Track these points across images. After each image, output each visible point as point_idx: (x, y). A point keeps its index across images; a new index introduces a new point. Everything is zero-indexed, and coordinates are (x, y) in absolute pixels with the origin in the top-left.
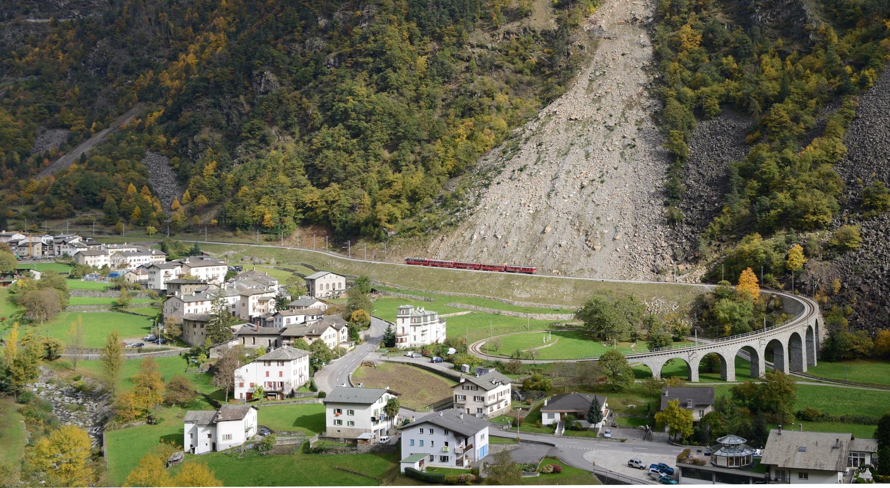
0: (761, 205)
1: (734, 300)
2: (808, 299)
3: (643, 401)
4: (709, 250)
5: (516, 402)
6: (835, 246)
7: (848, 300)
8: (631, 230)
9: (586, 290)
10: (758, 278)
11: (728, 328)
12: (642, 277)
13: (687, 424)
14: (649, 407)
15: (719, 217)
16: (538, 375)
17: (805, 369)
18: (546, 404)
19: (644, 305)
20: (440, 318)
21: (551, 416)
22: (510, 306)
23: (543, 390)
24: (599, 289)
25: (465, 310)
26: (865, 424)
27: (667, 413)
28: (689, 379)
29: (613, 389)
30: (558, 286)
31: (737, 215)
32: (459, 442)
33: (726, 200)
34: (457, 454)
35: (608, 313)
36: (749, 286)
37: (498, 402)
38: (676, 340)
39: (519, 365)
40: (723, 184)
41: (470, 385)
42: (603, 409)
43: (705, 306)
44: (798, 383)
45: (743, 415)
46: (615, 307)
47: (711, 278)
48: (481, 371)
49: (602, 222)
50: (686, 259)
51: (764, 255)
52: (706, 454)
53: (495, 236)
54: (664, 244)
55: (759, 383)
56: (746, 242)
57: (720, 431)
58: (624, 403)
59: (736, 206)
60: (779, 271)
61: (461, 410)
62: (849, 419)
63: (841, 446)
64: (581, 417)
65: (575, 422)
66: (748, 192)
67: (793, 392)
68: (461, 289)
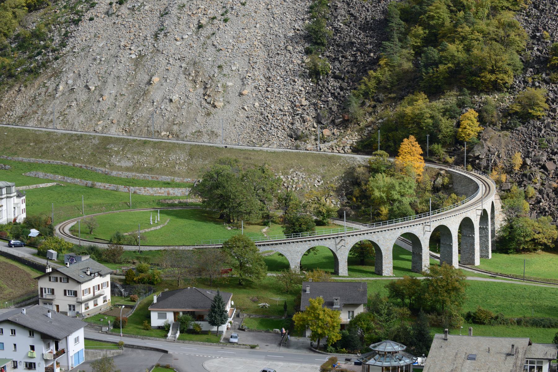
0: (427, 58)
1: (392, 175)
2: (483, 177)
3: (278, 299)
4: (362, 112)
5: (117, 298)
6: (516, 113)
7: (530, 179)
8: (262, 84)
9: (204, 158)
10: (423, 148)
11: (384, 210)
12: (276, 144)
13: (334, 327)
14: (285, 306)
15: (375, 71)
16: (144, 265)
17: (477, 262)
18: (155, 301)
19: (279, 179)
20: (17, 191)
21: (162, 316)
22: (107, 178)
23: (151, 284)
24: (221, 157)
25: (49, 181)
26: (544, 326)
27: (309, 313)
28: (336, 273)
29: (240, 284)
30: (168, 153)
31: (397, 69)
32: (48, 346)
33: (384, 50)
34: (46, 361)
35: (232, 188)
36: (411, 158)
37: (95, 297)
38: (319, 223)
39: (121, 252)
40: (380, 29)
41: (59, 277)
42: (228, 308)
43: (356, 182)
44: (469, 278)
45: (402, 317)
46: (242, 180)
47: (364, 147)
48: (71, 259)
49: (225, 72)
50: (333, 122)
51: (430, 121)
52: (356, 364)
53: (87, 87)
54: (304, 102)
55: (422, 278)
56: (409, 104)
57: (375, 336)
58: (254, 301)
59: (397, 57)
60: (448, 141)
61: (48, 306)
62: (527, 322)
63: (517, 352)
64: (200, 318)
65: (192, 324)
66: (412, 41)
67: (463, 290)
68: (44, 154)
